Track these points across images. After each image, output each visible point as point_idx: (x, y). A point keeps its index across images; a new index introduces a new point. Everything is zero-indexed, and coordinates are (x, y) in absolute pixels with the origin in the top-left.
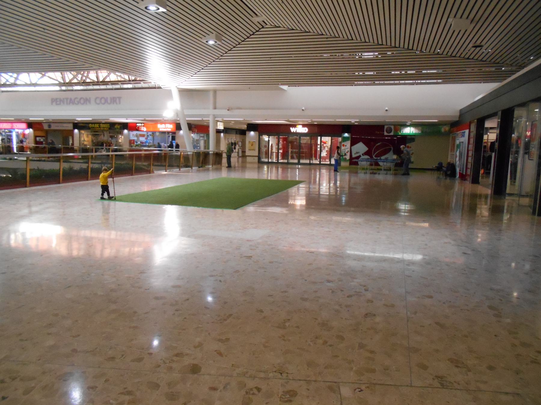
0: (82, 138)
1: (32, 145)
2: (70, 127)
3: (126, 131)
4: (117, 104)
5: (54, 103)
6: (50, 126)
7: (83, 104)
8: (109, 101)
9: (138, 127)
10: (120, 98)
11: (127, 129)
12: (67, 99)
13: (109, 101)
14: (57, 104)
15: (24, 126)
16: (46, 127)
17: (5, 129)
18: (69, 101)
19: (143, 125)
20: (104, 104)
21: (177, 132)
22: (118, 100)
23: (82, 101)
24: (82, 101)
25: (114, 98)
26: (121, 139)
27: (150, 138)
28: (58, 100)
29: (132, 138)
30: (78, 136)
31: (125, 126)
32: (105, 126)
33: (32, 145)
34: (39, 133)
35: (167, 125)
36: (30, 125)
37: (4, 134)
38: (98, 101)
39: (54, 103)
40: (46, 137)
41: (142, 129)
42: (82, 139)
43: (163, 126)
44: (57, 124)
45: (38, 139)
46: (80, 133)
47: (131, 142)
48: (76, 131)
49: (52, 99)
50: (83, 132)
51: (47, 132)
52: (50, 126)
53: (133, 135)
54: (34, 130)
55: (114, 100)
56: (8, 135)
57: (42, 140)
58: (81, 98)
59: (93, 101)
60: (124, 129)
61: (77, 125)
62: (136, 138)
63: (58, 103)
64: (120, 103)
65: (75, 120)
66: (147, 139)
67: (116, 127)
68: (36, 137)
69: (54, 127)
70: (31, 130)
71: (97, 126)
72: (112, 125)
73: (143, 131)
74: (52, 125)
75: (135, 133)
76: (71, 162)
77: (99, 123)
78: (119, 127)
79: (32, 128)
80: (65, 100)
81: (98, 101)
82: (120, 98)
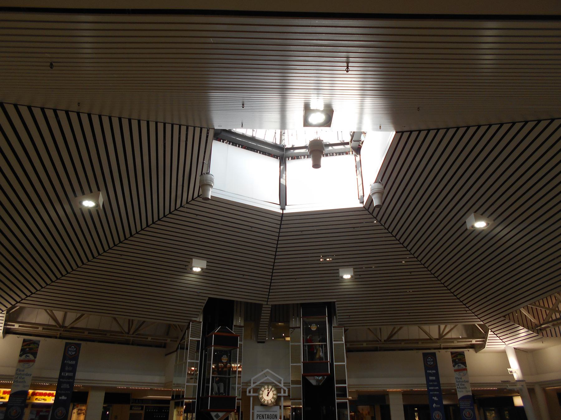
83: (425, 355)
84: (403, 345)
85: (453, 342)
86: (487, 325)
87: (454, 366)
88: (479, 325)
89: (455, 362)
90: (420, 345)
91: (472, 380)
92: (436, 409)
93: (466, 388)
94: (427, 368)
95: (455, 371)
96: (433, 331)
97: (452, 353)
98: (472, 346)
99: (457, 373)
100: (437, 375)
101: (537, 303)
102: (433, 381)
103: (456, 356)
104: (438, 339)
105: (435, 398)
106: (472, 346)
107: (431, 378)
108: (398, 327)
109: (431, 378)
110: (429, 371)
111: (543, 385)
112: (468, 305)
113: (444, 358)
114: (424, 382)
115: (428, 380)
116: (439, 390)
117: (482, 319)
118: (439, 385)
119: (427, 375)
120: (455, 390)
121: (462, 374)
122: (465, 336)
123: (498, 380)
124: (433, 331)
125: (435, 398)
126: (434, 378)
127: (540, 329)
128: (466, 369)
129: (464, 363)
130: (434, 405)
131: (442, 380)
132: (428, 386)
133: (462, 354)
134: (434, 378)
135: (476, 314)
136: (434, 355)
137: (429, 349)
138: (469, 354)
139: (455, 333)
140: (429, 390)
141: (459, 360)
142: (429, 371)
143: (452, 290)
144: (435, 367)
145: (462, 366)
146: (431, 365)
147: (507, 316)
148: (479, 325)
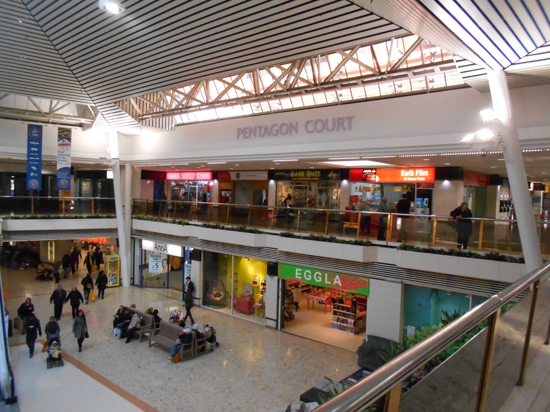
0: (278, 192)
1: (215, 203)
2: (264, 176)
3: (345, 182)
4: (344, 129)
5: (241, 136)
6: (238, 176)
7: (284, 134)
8: (330, 126)
9: (366, 176)
10: (350, 119)
11: (347, 178)
12: (260, 127)
13: (330, 126)
14: (245, 137)
15: (208, 175)
16: (233, 177)
17: (189, 181)
18: (263, 130)
19: (374, 171)
20: (321, 131)
21: (438, 182)
22: (346, 124)
23: (284, 129)
24: (284, 129)
25: (339, 119)
26: (335, 194)
27: (378, 193)
28: (248, 131)
29: (354, 193)
30: (274, 189)
31: (345, 173)
32: (313, 174)
33: (215, 203)
34: (225, 186)
35: (417, 171)
36: (215, 175)
37: (186, 186)
38: (311, 127)
39: (241, 136)
40: (233, 190)
41: (373, 179)
42: (280, 194)
43: (411, 173)
44: (249, 173)
45: (223, 193)
46: (277, 186)
47: (354, 199)
48: (272, 182)
49: (239, 130)
50: (281, 183)
51: (235, 183)
52: (238, 176)
53: (355, 188)
54: (220, 182)
55: (339, 124)
56: (192, 188)
57: (228, 195)
58: (282, 125)
59: (301, 128)
60: (342, 179)
61: (272, 174)
62: (360, 194)
63: (247, 135)
64: (350, 128)
65: (270, 163)
66: (373, 194)
67: (330, 175)
68: (221, 190)
69: (243, 177)
70: (216, 181)
71: (302, 174)
72: (325, 172)
73: (374, 183)
74: (241, 173)
75: (359, 184)
76: (261, 233)
77: (305, 171)
78: (334, 175)
79: (216, 179)
80: (258, 130)
81: (311, 127)
82: (350, 119)
83: (30, 127)
84: (6, 113)
85: (62, 118)
86: (99, 108)
87: (59, 141)
88: (91, 106)
89: (60, 137)
90: (27, 116)
91: (73, 155)
92: (33, 177)
93: (66, 161)
94: (30, 139)
95: (60, 145)
96: (44, 104)
97: (59, 129)
98: (81, 125)
99: (61, 147)
100: (40, 147)
101: (145, 97)
102: (34, 152)
103: (63, 132)
104: (47, 113)
105: (34, 168)
106: (81, 125)
107: (33, 149)
108: (4, 93)
109: (33, 149)
110: (32, 143)
111: (133, 164)
112: (84, 86)
113: (50, 133)
114: (25, 151)
115: (29, 151)
116: (40, 161)
117: (95, 102)
118: (40, 156)
119: (30, 146)
120: (56, 161)
121: (65, 148)
122: (76, 115)
123: (96, 156)
124: (44, 104)
125: (34, 168)
126: (36, 149)
127: (142, 119)
128: (69, 145)
129: (69, 139)
130: (32, 174)
131: (44, 152)
132: (29, 156)
133: (69, 131)
134: (36, 149)
135: (91, 96)
136: (40, 128)
137: (37, 122)
138: (76, 132)
139: (67, 110)
140: (29, 160)
141: (65, 135)
142: (32, 143)
143: (72, 68)
144: (40, 139)
145: (67, 141)
146: (35, 136)
147: (118, 103)
148: (91, 106)
